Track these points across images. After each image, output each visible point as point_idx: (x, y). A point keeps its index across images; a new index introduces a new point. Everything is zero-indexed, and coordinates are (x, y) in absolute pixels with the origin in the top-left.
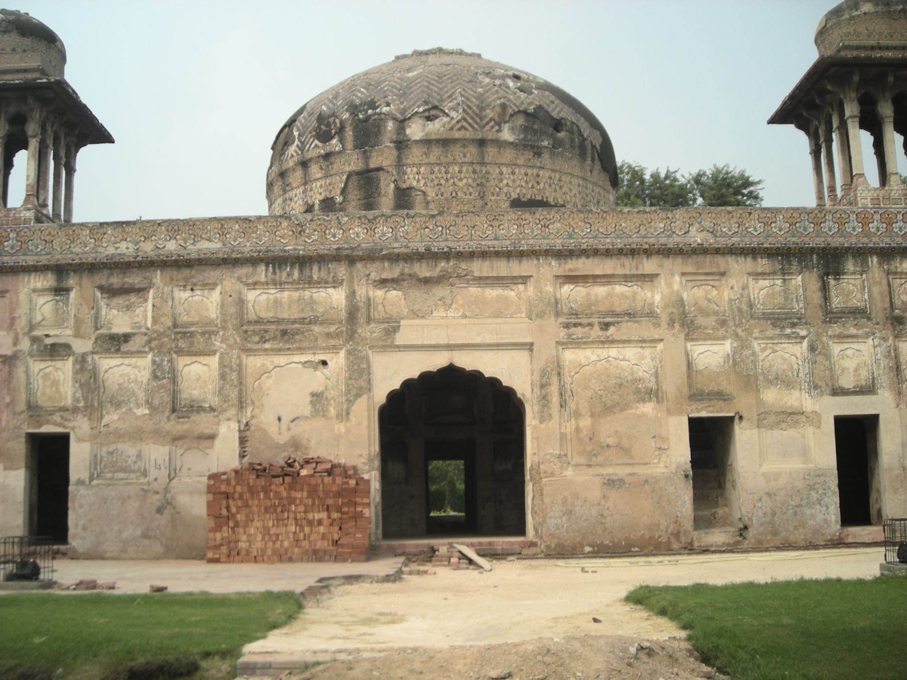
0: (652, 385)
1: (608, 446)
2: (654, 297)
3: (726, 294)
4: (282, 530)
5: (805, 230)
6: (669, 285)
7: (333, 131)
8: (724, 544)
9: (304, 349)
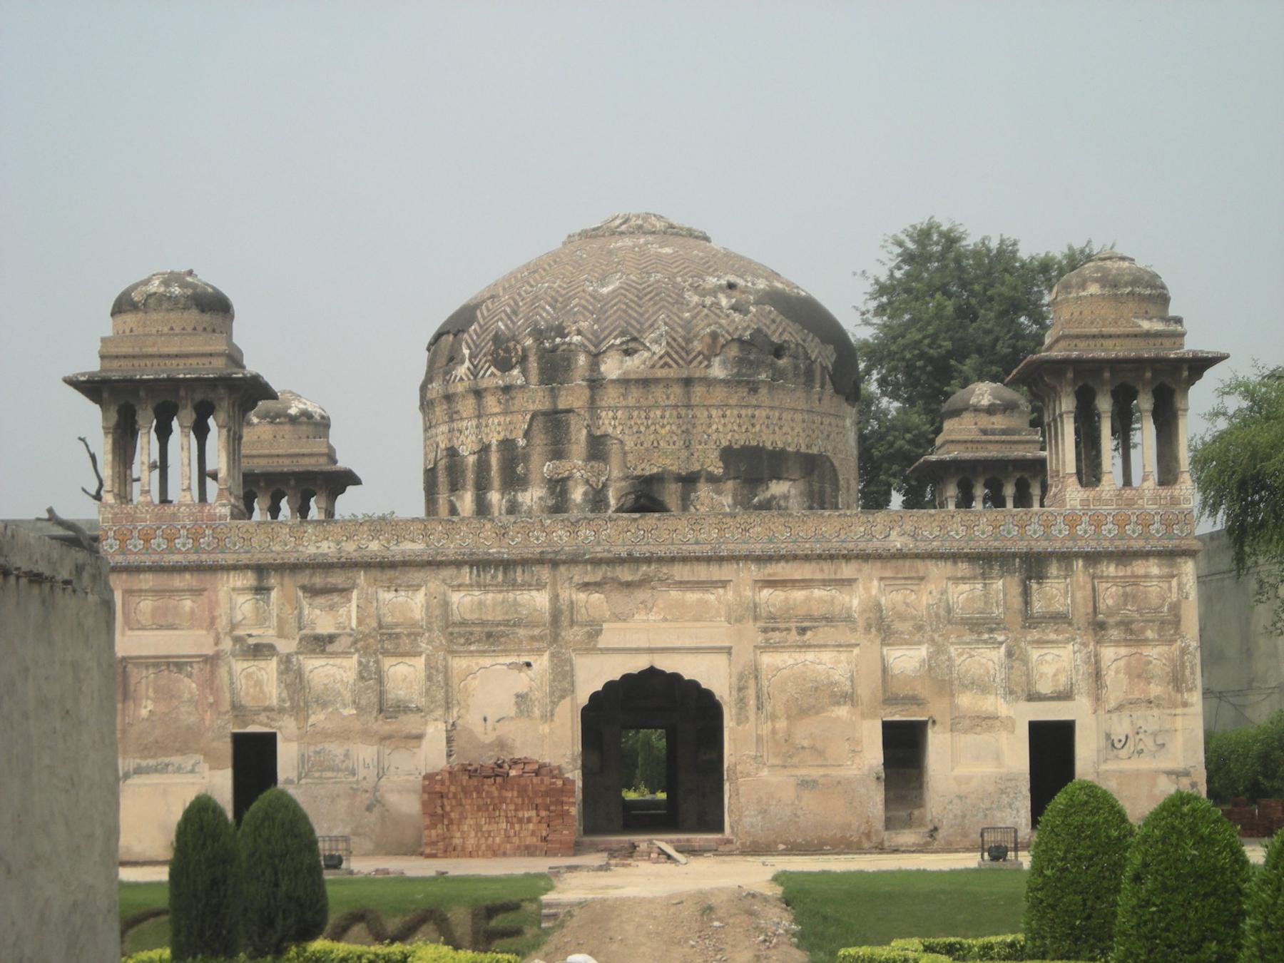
0: (848, 688)
1: (803, 748)
2: (854, 600)
3: (924, 598)
4: (494, 827)
5: (1009, 533)
6: (867, 589)
7: (514, 360)
8: (914, 844)
9: (510, 651)
